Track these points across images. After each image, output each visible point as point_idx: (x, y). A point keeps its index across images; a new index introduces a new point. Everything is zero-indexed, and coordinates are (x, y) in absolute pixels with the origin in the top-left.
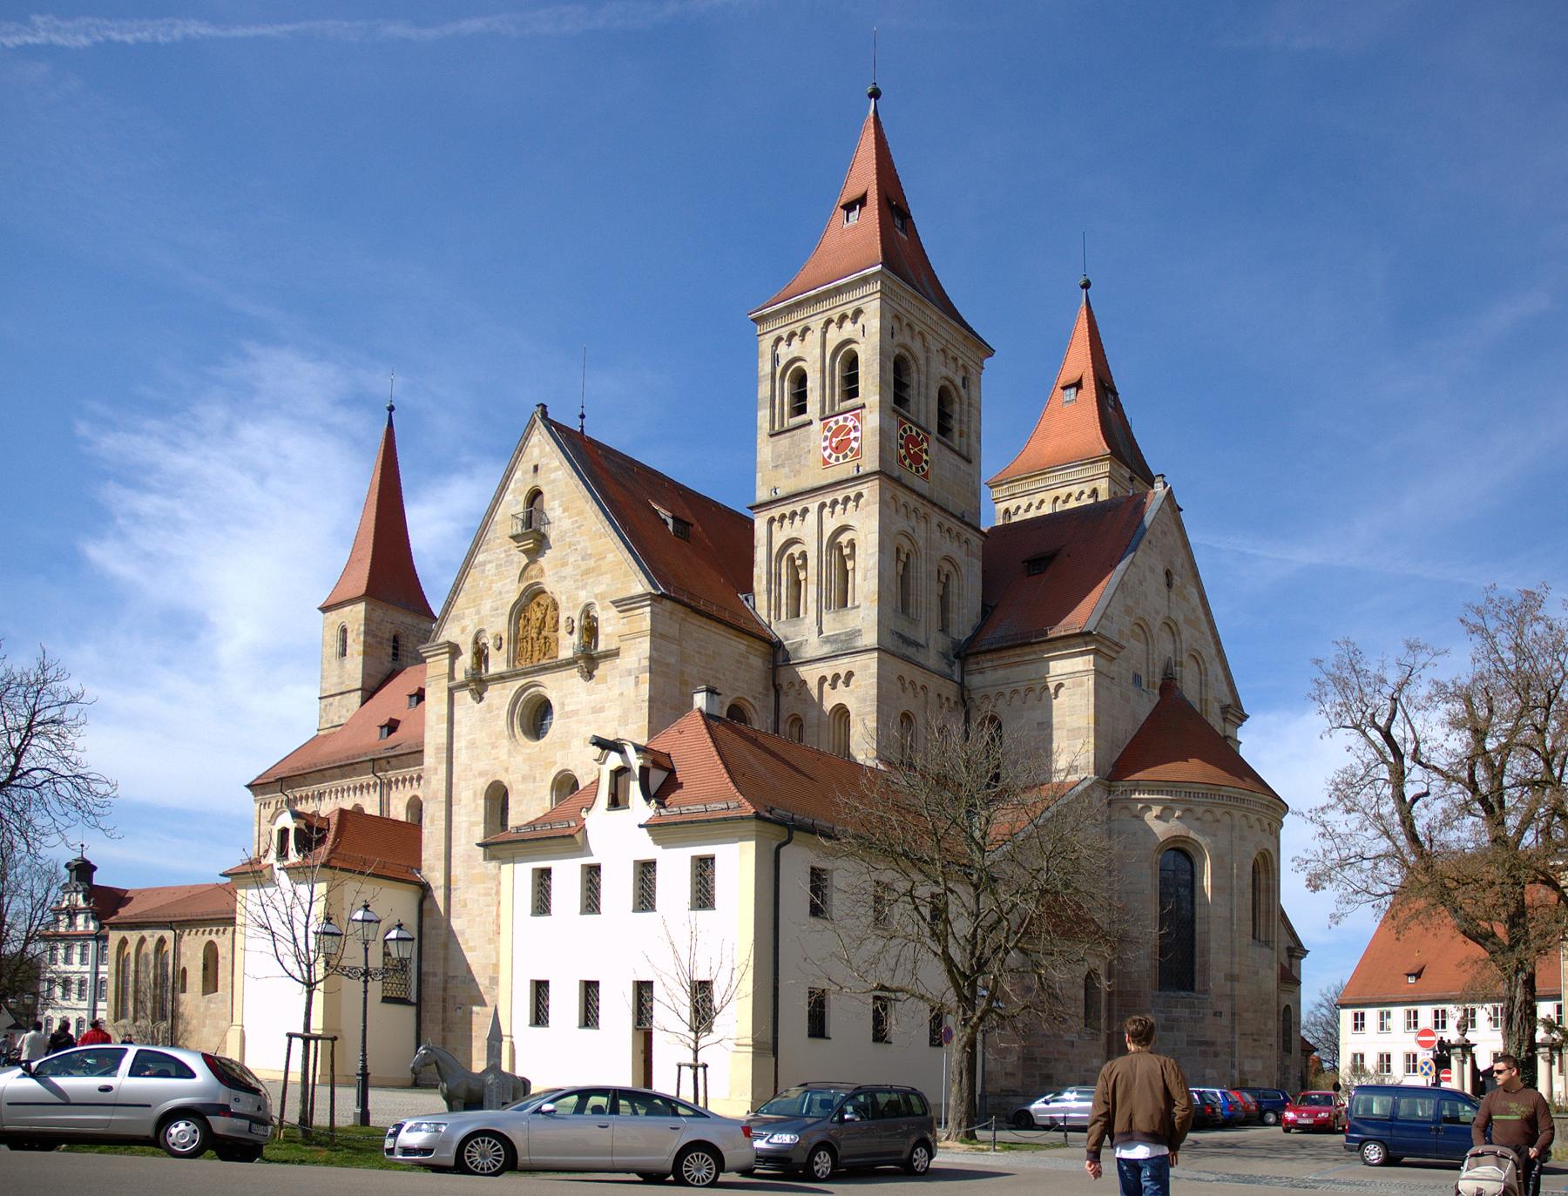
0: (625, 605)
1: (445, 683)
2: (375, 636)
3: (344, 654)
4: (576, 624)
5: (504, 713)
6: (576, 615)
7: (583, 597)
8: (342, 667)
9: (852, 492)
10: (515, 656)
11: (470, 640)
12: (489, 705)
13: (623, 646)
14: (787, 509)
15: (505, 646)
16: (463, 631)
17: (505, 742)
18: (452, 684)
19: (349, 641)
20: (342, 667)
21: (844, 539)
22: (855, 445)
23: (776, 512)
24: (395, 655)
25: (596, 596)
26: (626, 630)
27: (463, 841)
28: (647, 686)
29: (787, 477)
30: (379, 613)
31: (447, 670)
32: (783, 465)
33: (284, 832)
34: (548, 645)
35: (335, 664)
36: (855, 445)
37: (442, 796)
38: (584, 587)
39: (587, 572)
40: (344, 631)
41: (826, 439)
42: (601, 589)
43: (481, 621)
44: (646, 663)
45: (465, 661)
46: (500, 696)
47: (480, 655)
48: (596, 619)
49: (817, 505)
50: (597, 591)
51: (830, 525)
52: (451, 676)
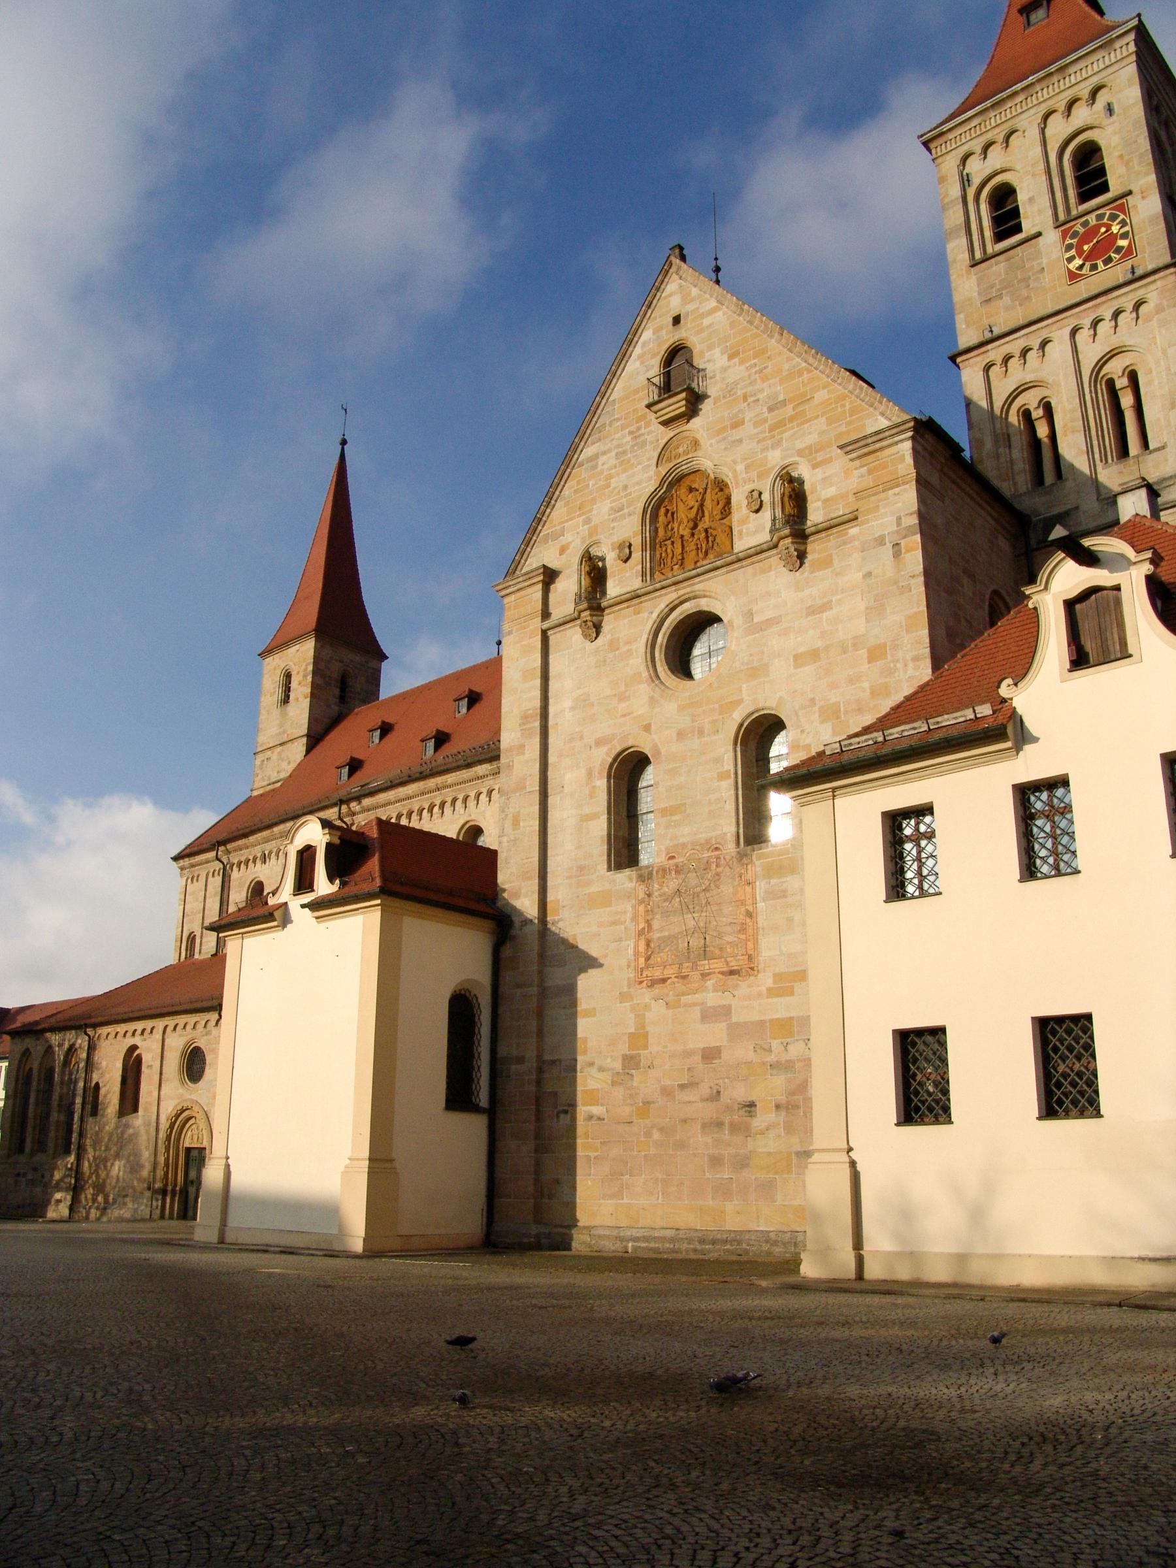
1: (537, 624)
2: (323, 676)
3: (286, 700)
4: (766, 497)
5: (640, 646)
6: (766, 486)
7: (775, 459)
8: (284, 715)
9: (1125, 299)
12: (613, 646)
14: (1014, 345)
15: (637, 555)
16: (562, 550)
17: (644, 690)
18: (546, 625)
19: (294, 685)
20: (284, 715)
21: (1115, 368)
22: (1123, 243)
23: (995, 353)
24: (342, 699)
25: (800, 453)
26: (869, 481)
27: (569, 846)
28: (919, 554)
29: (1007, 309)
30: (328, 652)
31: (539, 606)
32: (1000, 297)
33: (306, 855)
35: (276, 712)
36: (1123, 243)
37: (534, 785)
38: (777, 444)
39: (780, 424)
40: (288, 676)
41: (1069, 248)
42: (811, 439)
43: (593, 531)
44: (914, 520)
45: (568, 588)
46: (633, 629)
47: (596, 575)
48: (801, 482)
49: (1067, 331)
50: (799, 445)
51: (1091, 353)
52: (546, 614)
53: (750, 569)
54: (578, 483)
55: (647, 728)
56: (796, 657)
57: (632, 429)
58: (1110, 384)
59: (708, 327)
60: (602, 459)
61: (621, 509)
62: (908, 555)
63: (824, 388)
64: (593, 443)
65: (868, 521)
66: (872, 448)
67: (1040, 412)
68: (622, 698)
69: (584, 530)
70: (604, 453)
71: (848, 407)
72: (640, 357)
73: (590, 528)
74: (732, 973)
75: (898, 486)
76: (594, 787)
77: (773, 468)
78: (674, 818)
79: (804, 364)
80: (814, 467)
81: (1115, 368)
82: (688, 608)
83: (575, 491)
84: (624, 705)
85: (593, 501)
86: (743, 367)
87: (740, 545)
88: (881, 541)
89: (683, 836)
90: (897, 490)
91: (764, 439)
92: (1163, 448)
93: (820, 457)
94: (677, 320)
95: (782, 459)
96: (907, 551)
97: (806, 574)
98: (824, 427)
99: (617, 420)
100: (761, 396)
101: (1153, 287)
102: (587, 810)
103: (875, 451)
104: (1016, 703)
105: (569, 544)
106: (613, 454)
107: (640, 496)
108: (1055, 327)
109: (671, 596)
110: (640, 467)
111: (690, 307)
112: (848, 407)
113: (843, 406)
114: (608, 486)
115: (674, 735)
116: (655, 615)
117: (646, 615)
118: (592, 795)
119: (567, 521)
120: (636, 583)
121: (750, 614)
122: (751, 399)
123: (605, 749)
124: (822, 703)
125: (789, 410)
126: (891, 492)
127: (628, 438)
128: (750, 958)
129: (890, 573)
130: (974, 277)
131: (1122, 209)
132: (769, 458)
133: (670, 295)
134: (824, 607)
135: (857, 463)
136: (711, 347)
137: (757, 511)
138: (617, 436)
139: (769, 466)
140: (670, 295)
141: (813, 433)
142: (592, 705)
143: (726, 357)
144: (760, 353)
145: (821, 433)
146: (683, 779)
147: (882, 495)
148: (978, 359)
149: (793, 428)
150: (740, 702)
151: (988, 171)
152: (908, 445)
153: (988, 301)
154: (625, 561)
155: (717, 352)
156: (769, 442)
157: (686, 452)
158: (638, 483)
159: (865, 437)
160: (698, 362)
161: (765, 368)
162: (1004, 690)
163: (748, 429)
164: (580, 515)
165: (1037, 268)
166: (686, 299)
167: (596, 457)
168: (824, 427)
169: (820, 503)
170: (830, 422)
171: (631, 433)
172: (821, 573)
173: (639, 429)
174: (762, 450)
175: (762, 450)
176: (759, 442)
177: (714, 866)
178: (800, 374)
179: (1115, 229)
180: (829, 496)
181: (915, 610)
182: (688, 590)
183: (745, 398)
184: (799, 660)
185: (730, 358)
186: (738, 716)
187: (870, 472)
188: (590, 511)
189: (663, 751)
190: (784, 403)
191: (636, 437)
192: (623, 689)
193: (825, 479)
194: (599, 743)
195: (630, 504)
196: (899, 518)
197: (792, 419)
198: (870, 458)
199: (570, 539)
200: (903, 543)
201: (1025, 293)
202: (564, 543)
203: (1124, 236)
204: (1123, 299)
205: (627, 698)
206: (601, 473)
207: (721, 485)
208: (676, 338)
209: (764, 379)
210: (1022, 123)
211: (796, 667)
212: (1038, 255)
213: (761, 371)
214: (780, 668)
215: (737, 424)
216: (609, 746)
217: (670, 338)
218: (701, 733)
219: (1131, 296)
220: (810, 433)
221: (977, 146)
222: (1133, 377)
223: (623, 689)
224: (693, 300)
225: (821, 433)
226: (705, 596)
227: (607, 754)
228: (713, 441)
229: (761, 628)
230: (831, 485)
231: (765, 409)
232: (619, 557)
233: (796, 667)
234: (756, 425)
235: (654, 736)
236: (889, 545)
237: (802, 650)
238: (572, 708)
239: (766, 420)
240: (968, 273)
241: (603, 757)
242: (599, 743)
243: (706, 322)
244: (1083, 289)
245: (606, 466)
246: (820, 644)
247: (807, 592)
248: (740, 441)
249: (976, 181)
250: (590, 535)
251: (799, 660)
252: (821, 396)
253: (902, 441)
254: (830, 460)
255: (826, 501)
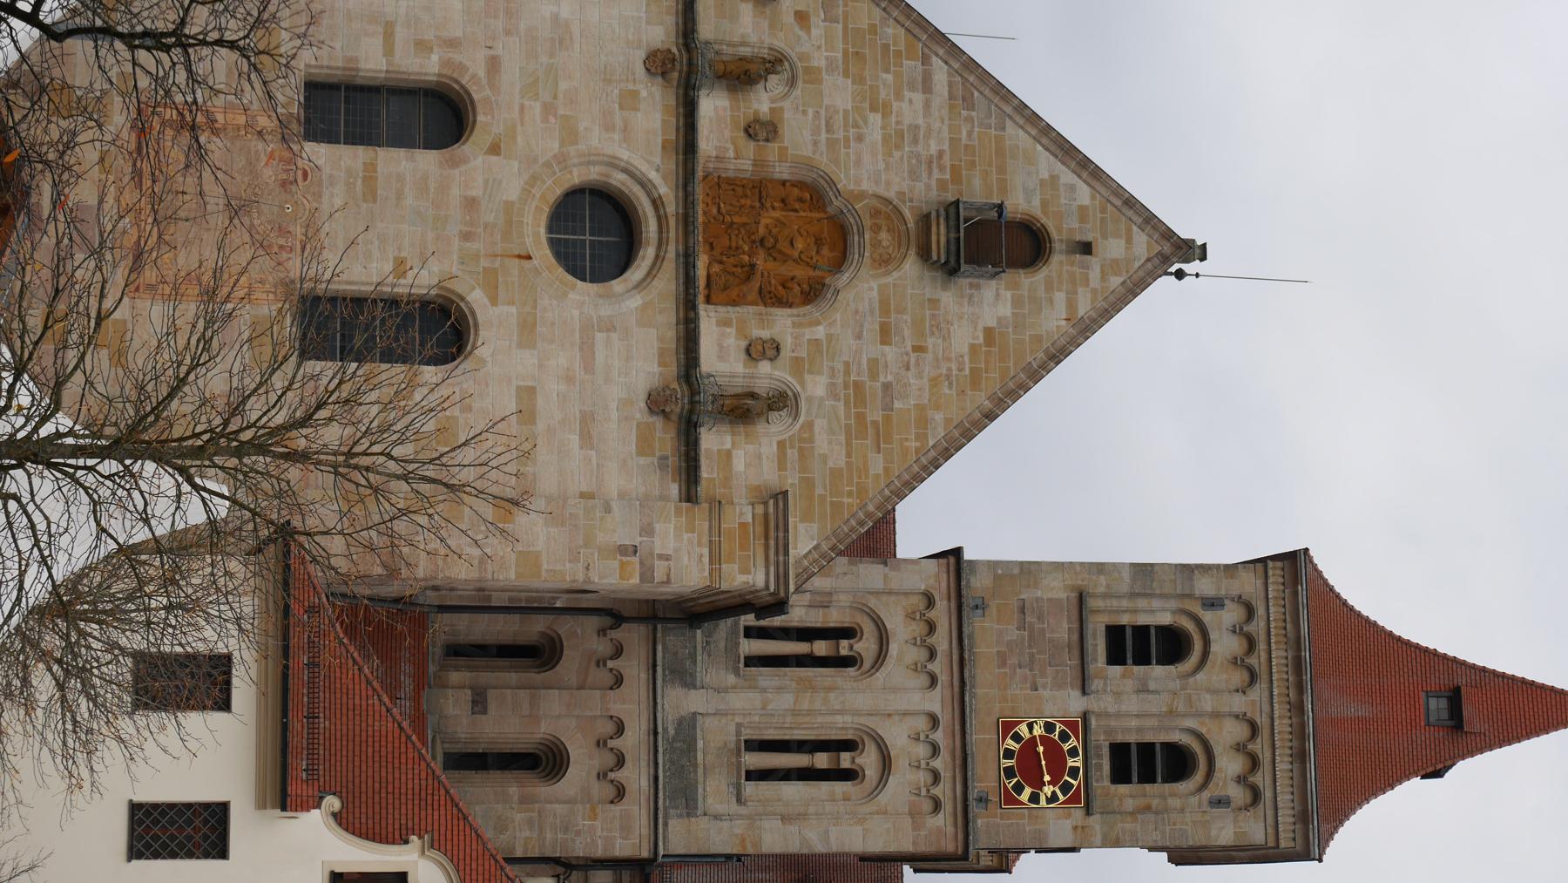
0: (775, 509)
4: (765, 367)
7: (815, 387)
10: (723, 185)
11: (780, 44)
13: (701, 512)
16: (802, 17)
25: (809, 426)
32: (1022, 626)
34: (738, 283)
43: (813, 76)
49: (936, 708)
50: (820, 424)
51: (897, 737)
53: (671, 334)
54: (898, 54)
55: (495, 149)
56: (531, 391)
57: (947, 159)
58: (848, 745)
59: (1051, 301)
60: (918, 98)
61: (829, 129)
62: (616, 564)
63: (886, 470)
64: (950, 85)
65: (678, 512)
66: (772, 534)
67: (844, 652)
68: (548, 109)
69: (819, 61)
70: (927, 105)
71: (846, 500)
72: (1054, 178)
73: (819, 70)
74: (138, 256)
75: (711, 562)
76: (431, 50)
77: (802, 383)
78: (359, 181)
79: (931, 443)
80: (781, 444)
81: (868, 760)
82: (651, 228)
83: (886, 47)
84: (537, 107)
85: (860, 80)
86: (966, 349)
87: (709, 321)
88: (648, 530)
89: (332, 195)
90: (706, 560)
91: (847, 372)
92: (739, 801)
93: (792, 454)
94: (1086, 248)
95: (809, 399)
96: (622, 564)
97: (638, 416)
98: (830, 464)
99: (970, 134)
100: (910, 374)
101: (950, 821)
102: (400, 34)
103: (767, 538)
104: (315, 812)
105: (808, 31)
106: (920, 121)
107: (837, 162)
108: (947, 693)
109: (671, 208)
110: (882, 166)
111: (1095, 275)
112: (846, 500)
113: (850, 494)
114: (873, 109)
115: (473, 193)
116: (653, 175)
117: (657, 160)
118: (422, 46)
119: (845, 29)
120: (708, 142)
121: (611, 328)
122: (913, 357)
123: (482, 73)
124: (461, 421)
125: (875, 415)
126: (706, 551)
127: (933, 150)
128: (151, 287)
129: (601, 538)
130: (1063, 595)
131: (1075, 799)
132: (818, 378)
133: (1129, 241)
134: (586, 438)
135: (760, 509)
136: (1017, 302)
137: (748, 351)
138: (945, 134)
139: (807, 377)
140: (1129, 241)
141: (829, 447)
142: (552, 55)
143: (992, 323)
144: (975, 379)
145: (824, 458)
146: (409, 201)
147: (705, 539)
148: (944, 585)
149: (847, 417)
150: (494, 301)
151: (1213, 636)
152: (760, 580)
153: (1022, 610)
154: (746, 131)
155: (1005, 310)
156: (840, 380)
157: (876, 244)
158: (858, 162)
159: (786, 530)
160: (1010, 275)
161: (950, 384)
162: (332, 802)
163: (872, 349)
164: (845, 52)
165: (1040, 681)
166: (1113, 266)
167: (927, 86)
168: (830, 464)
169: (728, 446)
170: (835, 474)
171: (941, 154)
172: (634, 438)
173: (942, 169)
174: (832, 369)
175: (832, 369)
176: (847, 364)
177: (282, 242)
178: (921, 437)
179: (1048, 790)
180: (735, 461)
181: (545, 567)
182: (672, 234)
183: (919, 349)
184: (527, 394)
185: (988, 332)
186: (476, 298)
187: (743, 525)
188: (846, 74)
189: (457, 172)
190: (888, 408)
191: (931, 162)
192: (561, 112)
193: (759, 457)
194: (494, 64)
195: (831, 144)
196: (667, 558)
197: (860, 417)
198: (760, 529)
199: (814, 32)
200: (636, 560)
201: (1013, 661)
202: (813, 19)
203: (1034, 798)
204: (948, 785)
205: (545, 120)
206: (899, 96)
207: (813, 293)
208: (1057, 246)
209: (935, 382)
210: (1258, 693)
211: (519, 388)
212: (1059, 685)
213: (948, 377)
214: (524, 363)
215: (885, 335)
216: (484, 81)
217: (1060, 230)
218: (467, 237)
219: (949, 793)
220: (830, 443)
221: (1257, 627)
222: (848, 775)
223: (561, 112)
224: (1104, 277)
225: (824, 458)
226: (657, 257)
227: (474, 76)
228: (875, 293)
229: (587, 348)
230: (747, 465)
231: (890, 378)
232: (757, 121)
233: (519, 388)
234: (874, 365)
235: (480, 159)
236: (637, 540)
237: (540, 401)
238: (555, 18)
239: (874, 376)
240: (1073, 588)
241: (472, 72)
242: (494, 64)
243: (1060, 297)
244: (982, 736)
245: (905, 105)
246: (541, 426)
247: (614, 415)
248: (859, 337)
249: (1207, 617)
250: (808, 70)
251: (527, 394)
252: (877, 464)
253: (767, 574)
254: (782, 465)
255: (729, 454)
